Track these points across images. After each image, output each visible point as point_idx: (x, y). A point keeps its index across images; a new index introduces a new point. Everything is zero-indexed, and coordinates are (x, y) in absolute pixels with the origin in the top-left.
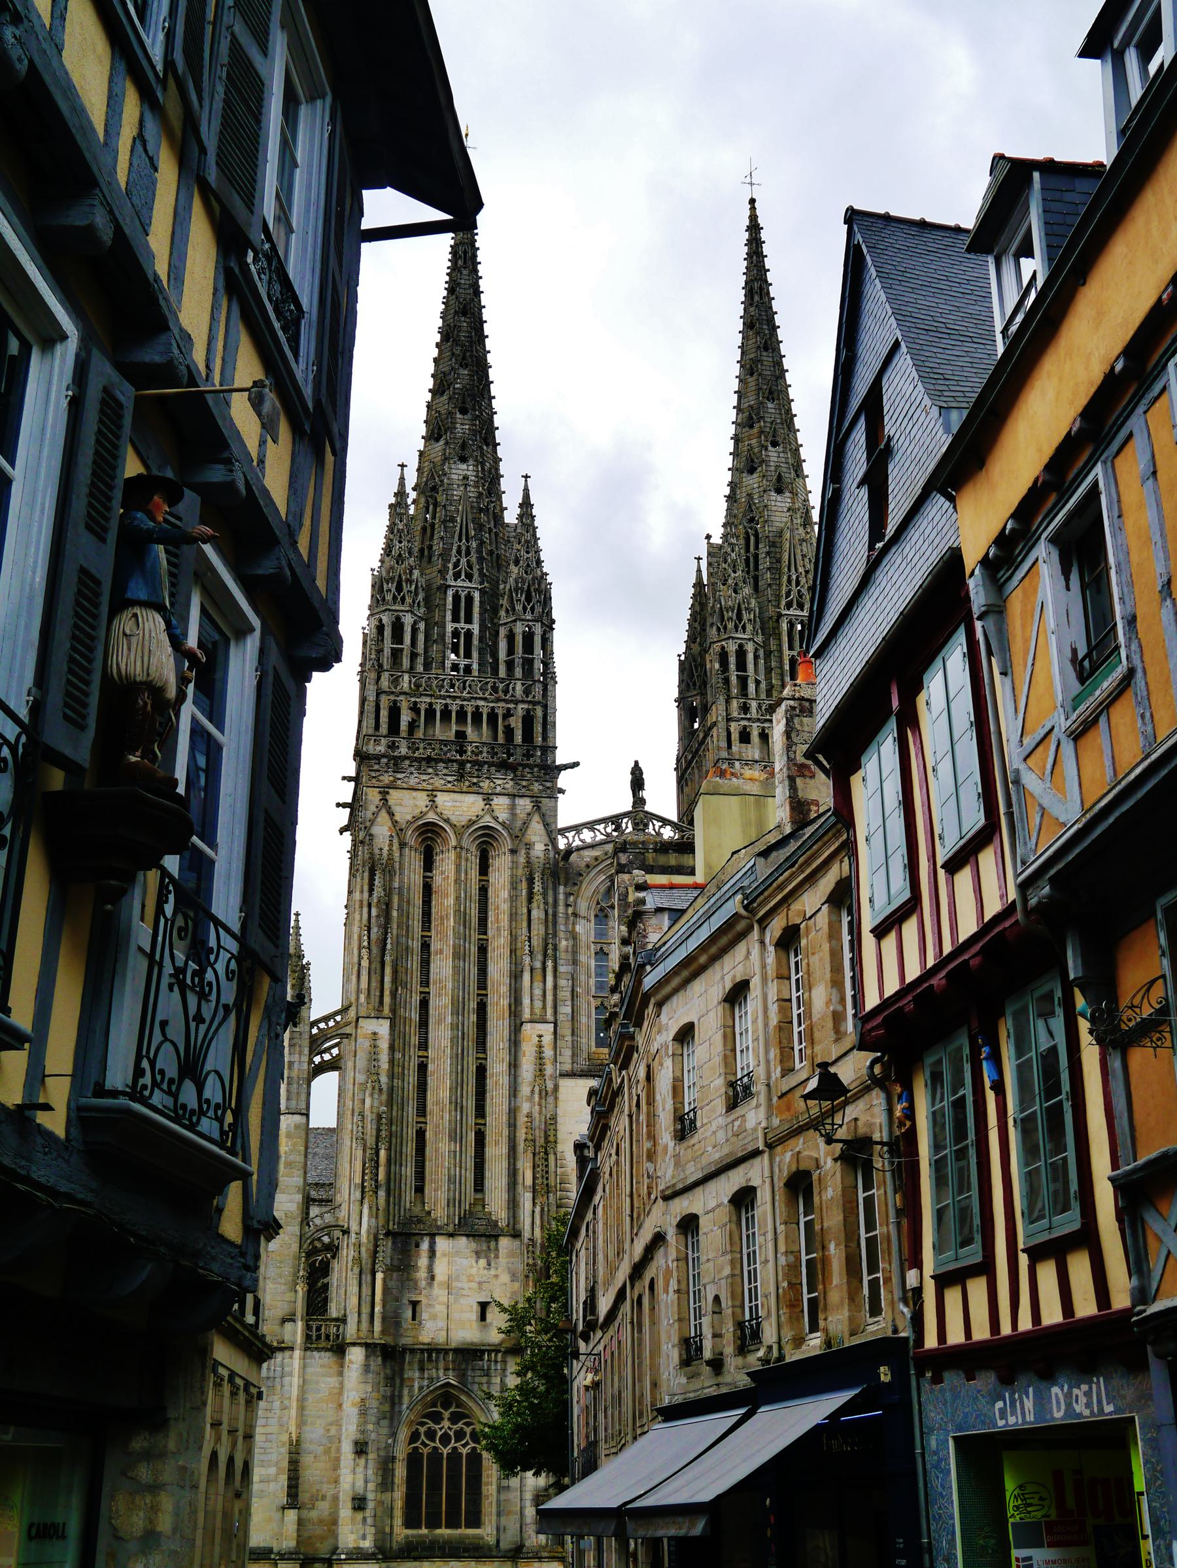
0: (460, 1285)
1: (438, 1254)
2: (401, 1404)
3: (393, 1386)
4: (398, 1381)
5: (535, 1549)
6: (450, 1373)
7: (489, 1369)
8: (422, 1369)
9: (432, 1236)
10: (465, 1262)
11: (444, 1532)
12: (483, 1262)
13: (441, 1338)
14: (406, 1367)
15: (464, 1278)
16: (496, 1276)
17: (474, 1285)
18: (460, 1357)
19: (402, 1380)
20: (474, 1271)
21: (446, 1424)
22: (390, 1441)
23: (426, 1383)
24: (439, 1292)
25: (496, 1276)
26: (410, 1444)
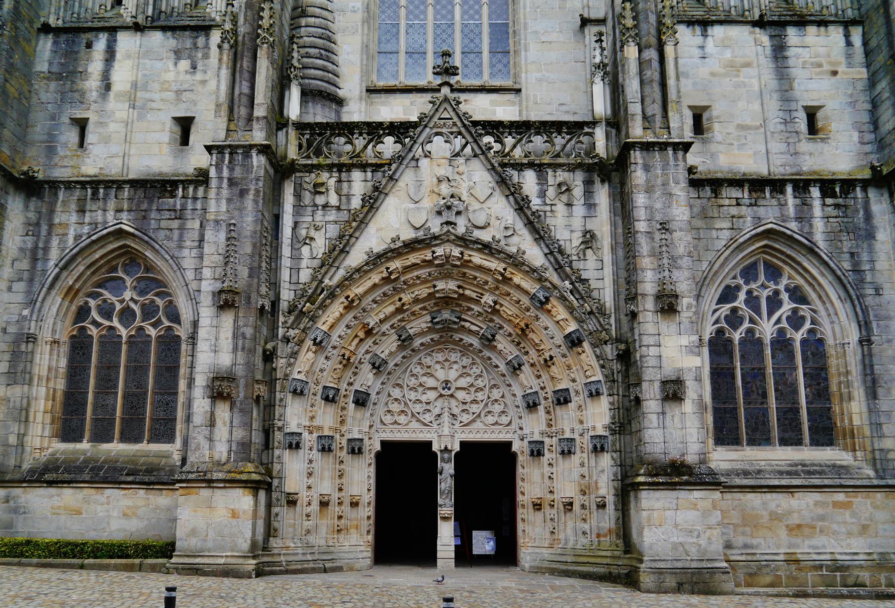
0: (147, 95)
1: (118, 56)
2: (46, 260)
3: (37, 235)
4: (44, 228)
5: (203, 467)
6: (124, 216)
7: (183, 209)
8: (82, 211)
9: (113, 31)
10: (158, 65)
11: (116, 448)
12: (185, 64)
13: (114, 170)
14: (59, 207)
15: (156, 86)
16: (204, 82)
17: (171, 95)
18: (140, 193)
19: (51, 226)
20: (170, 76)
21: (128, 295)
22: (26, 312)
23: (86, 229)
24: (116, 106)
25: (204, 82)
26: (75, 323)
